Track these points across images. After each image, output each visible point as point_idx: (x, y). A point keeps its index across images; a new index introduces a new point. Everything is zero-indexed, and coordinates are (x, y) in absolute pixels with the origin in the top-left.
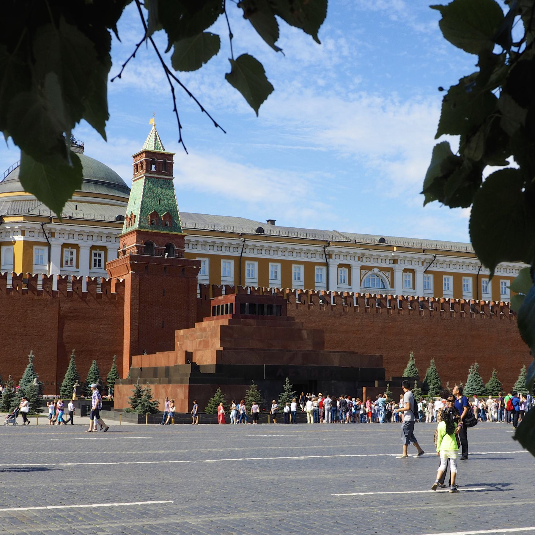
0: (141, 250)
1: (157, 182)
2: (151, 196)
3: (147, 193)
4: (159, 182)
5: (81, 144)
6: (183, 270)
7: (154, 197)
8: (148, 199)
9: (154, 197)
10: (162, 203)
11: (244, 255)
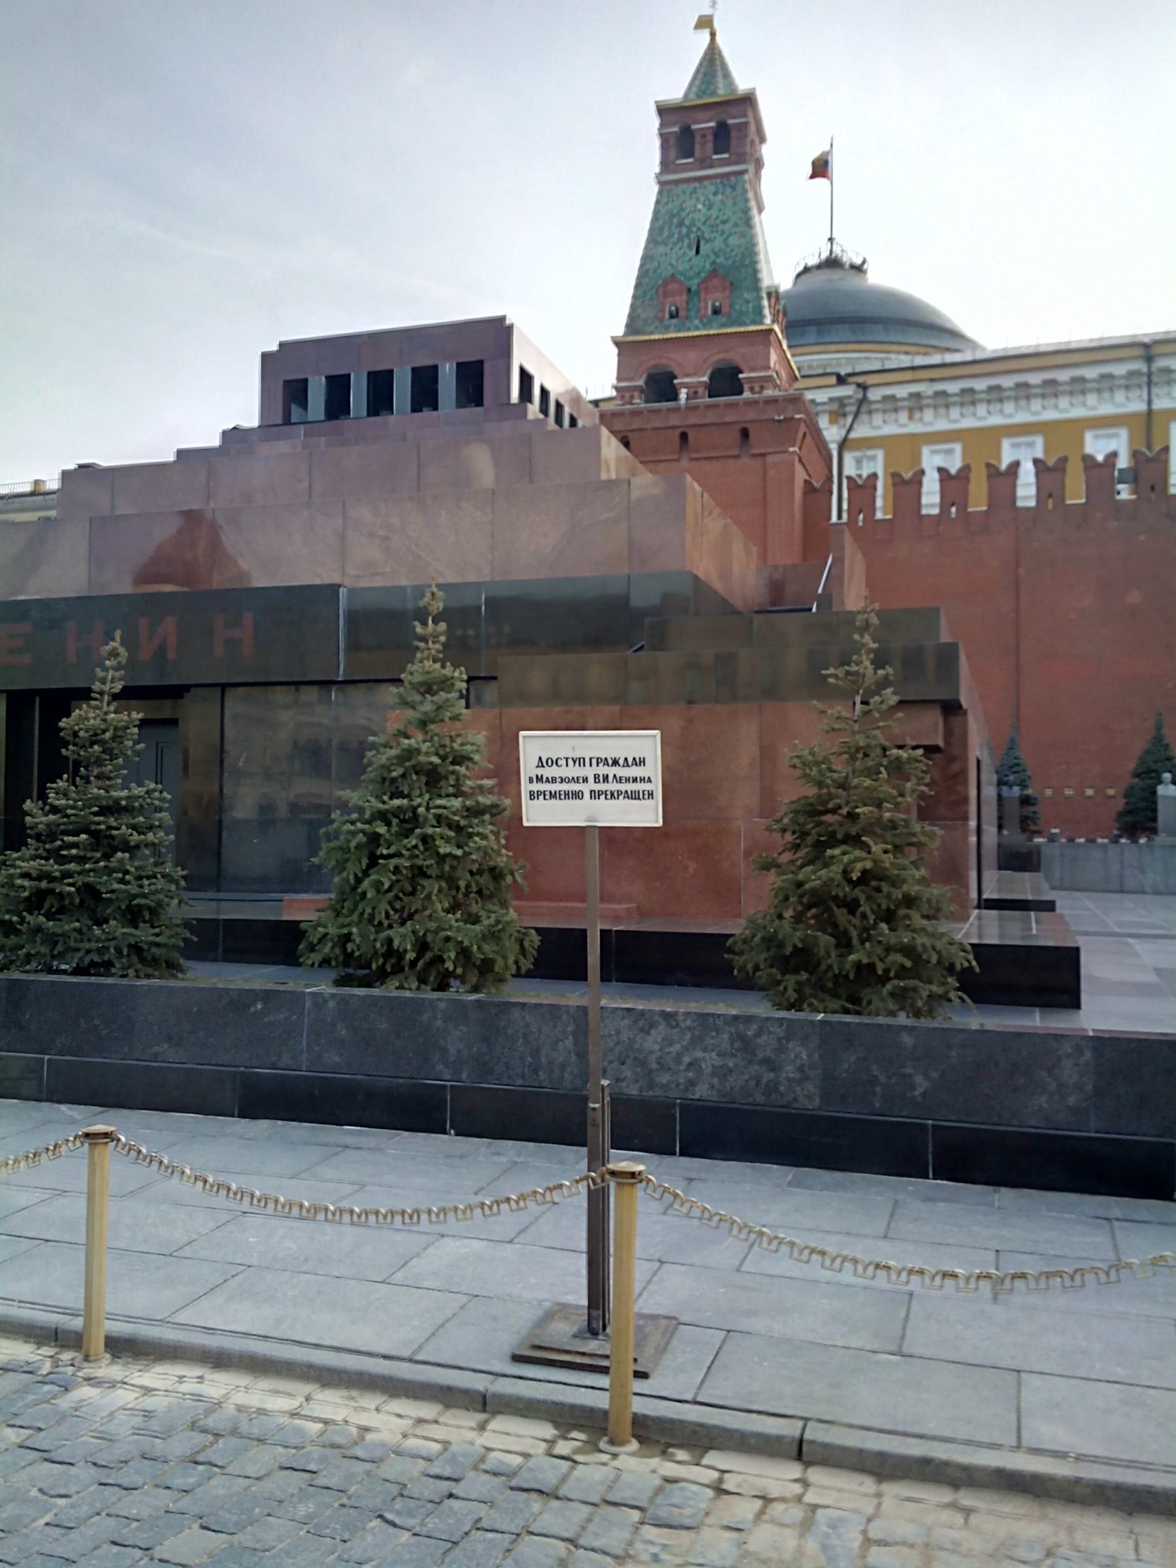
0: (632, 397)
1: (694, 191)
2: (671, 235)
3: (661, 230)
4: (700, 192)
5: (858, 261)
6: (745, 433)
7: (680, 239)
8: (661, 249)
9: (680, 239)
10: (704, 248)
11: (1157, 405)
